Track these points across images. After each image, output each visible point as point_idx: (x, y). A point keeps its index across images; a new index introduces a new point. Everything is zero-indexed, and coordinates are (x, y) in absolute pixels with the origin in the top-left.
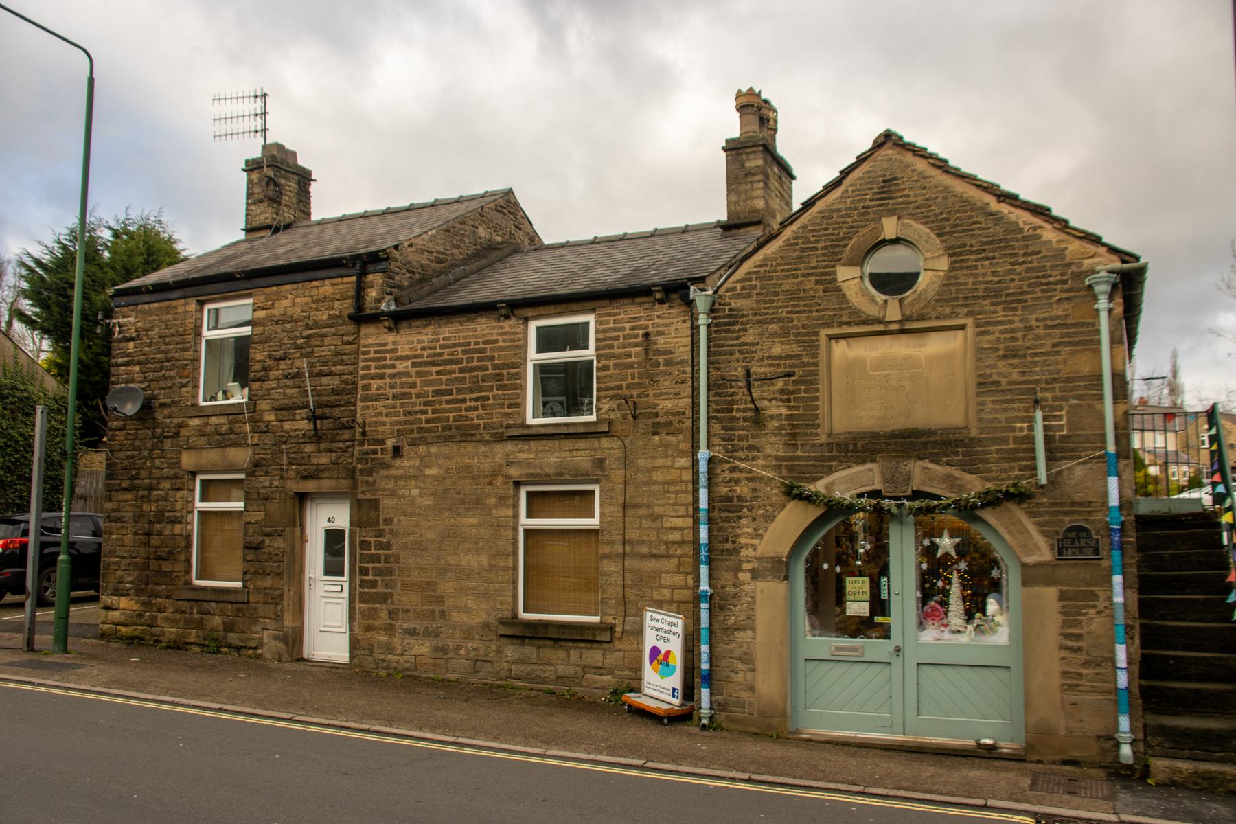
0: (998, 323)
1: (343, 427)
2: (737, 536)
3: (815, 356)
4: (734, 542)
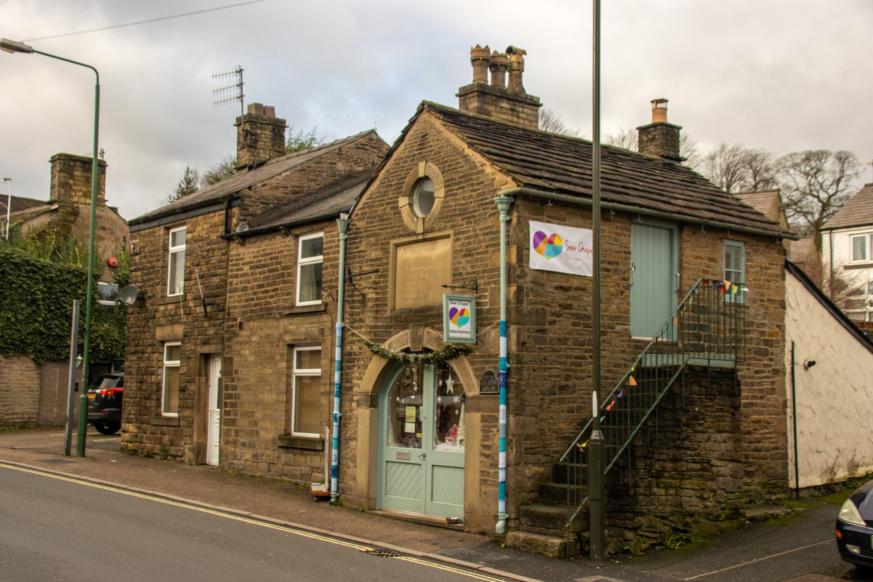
0: (464, 232)
1: (220, 311)
2: (352, 378)
3: (387, 258)
4: (351, 382)
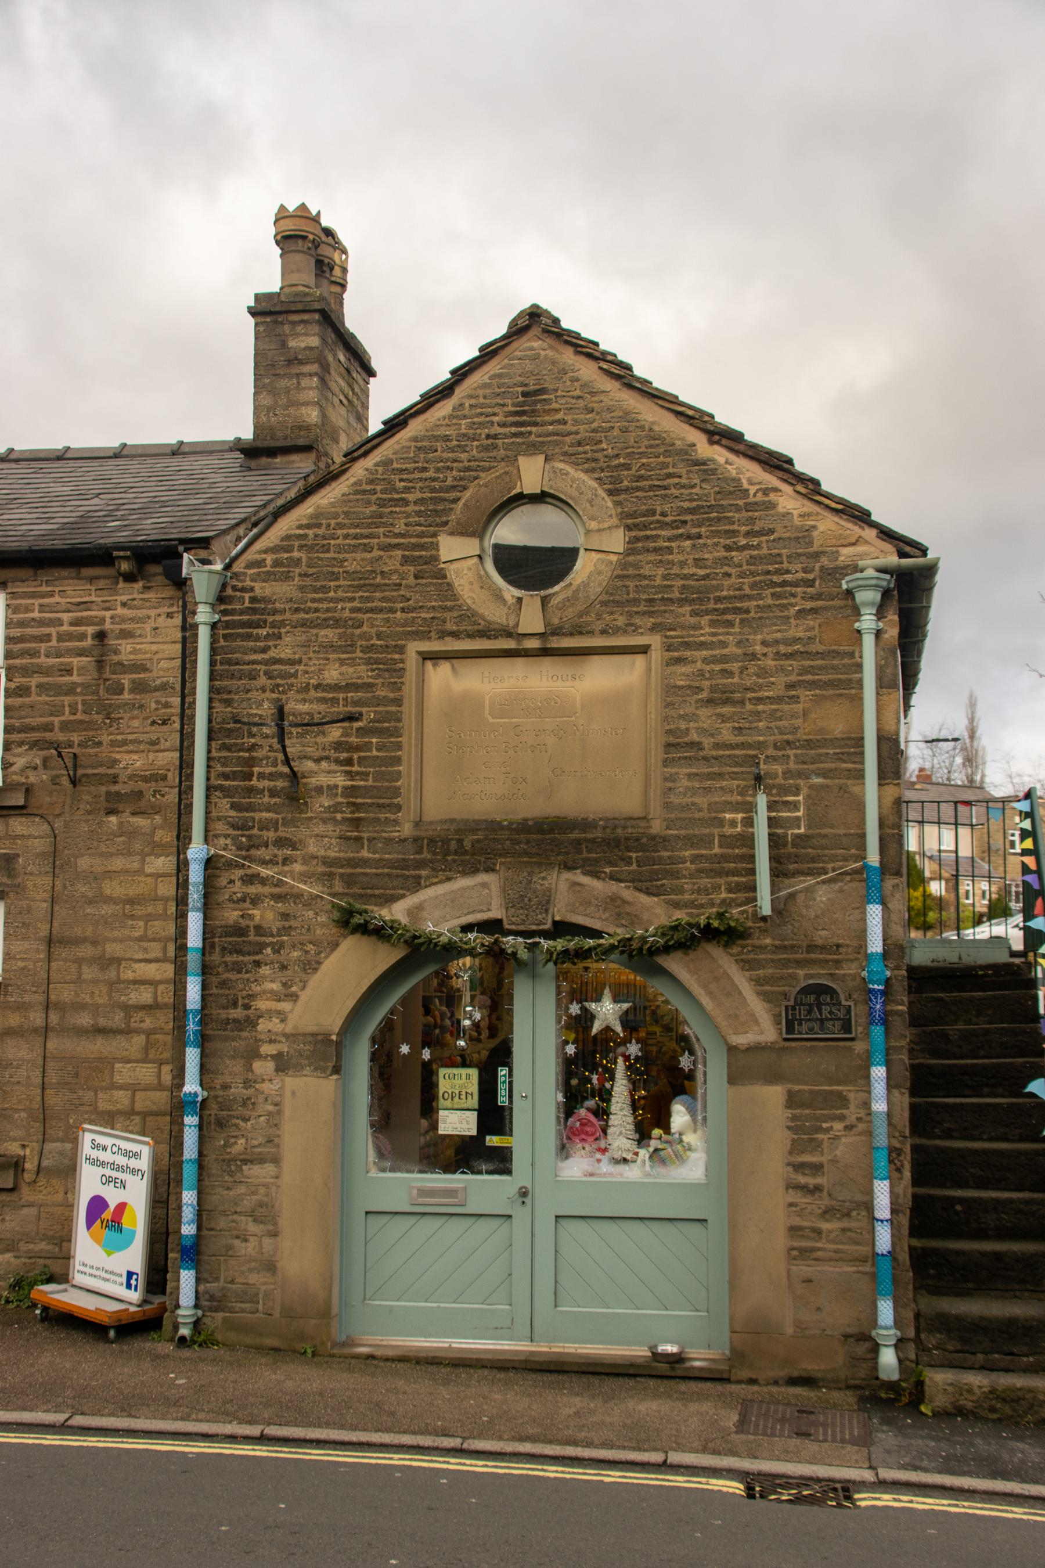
0: (702, 645)
2: (252, 997)
3: (397, 687)
4: (247, 1007)
